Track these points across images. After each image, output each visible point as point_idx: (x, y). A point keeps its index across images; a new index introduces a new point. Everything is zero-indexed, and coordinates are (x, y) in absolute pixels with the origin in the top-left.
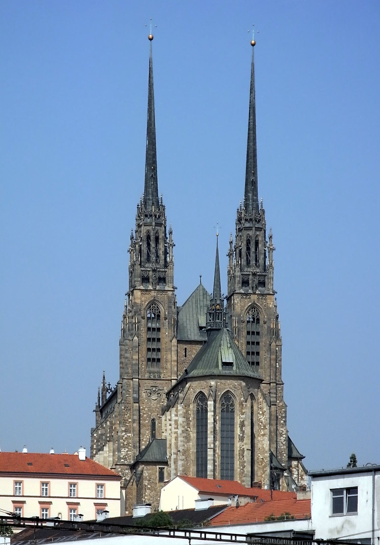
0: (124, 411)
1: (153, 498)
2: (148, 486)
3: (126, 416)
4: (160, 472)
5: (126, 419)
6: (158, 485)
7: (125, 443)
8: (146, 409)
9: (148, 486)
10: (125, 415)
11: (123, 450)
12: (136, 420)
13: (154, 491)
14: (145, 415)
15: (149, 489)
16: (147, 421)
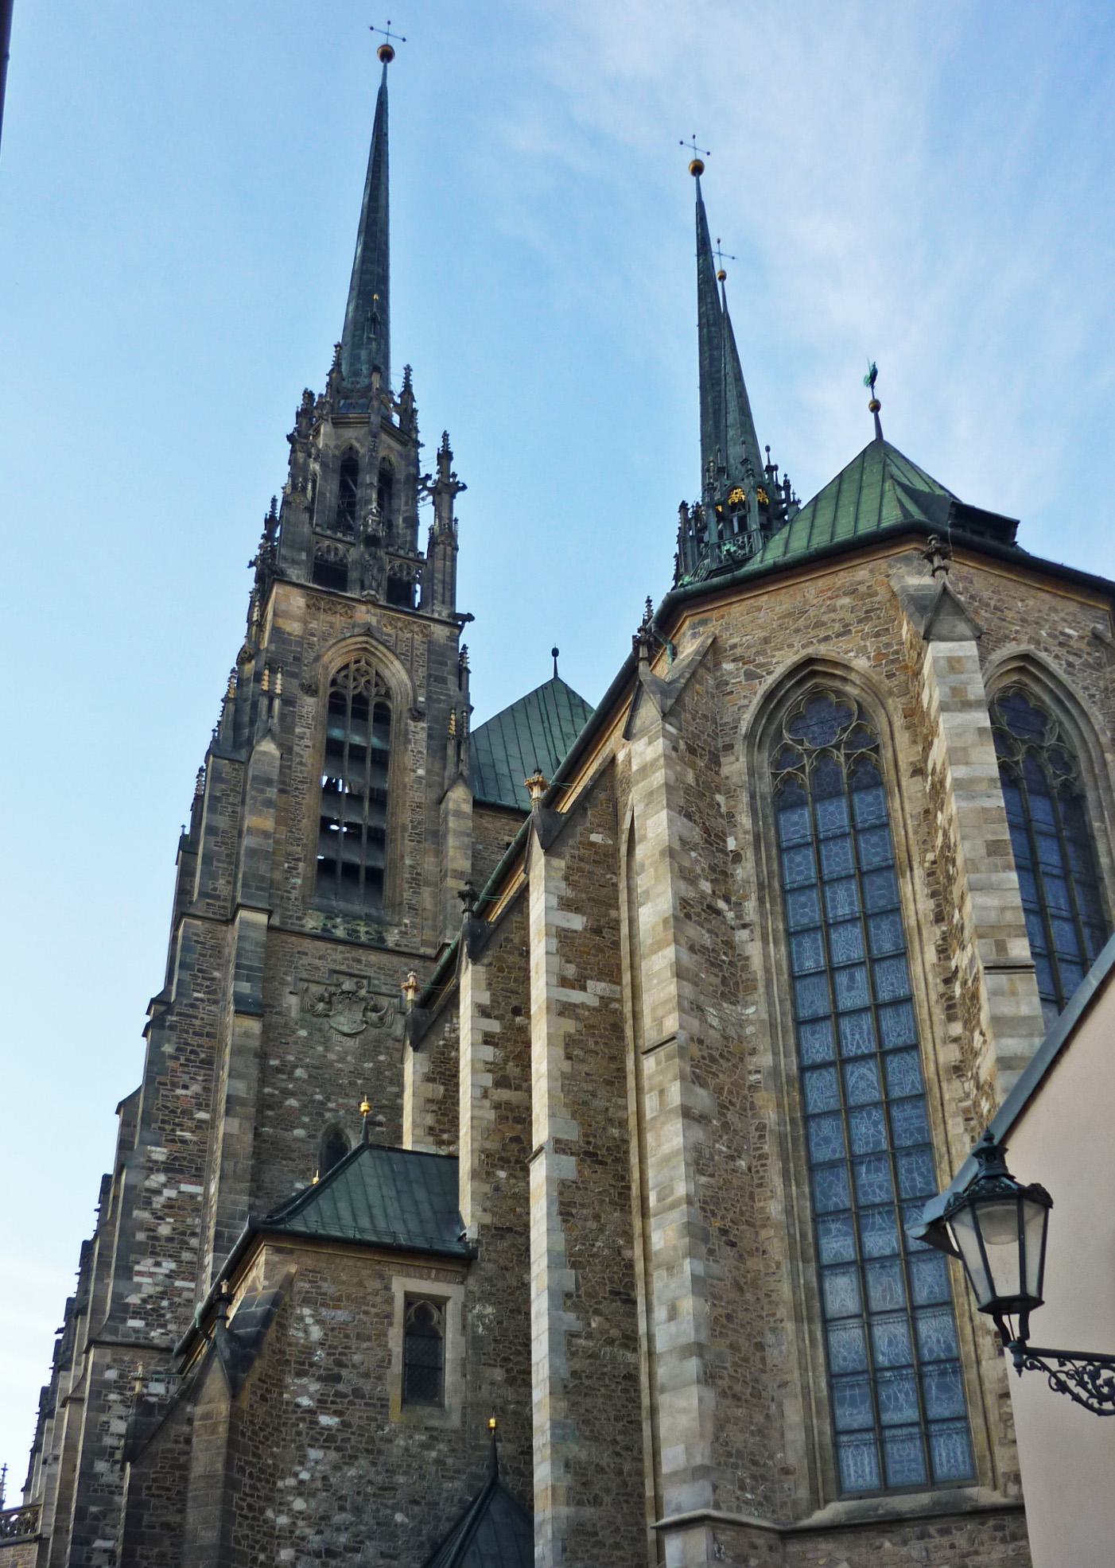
0: (170, 1064)
1: (357, 1511)
2: (325, 1420)
3: (179, 1092)
4: (409, 1332)
5: (183, 1105)
6: (395, 1414)
7: (164, 1230)
8: (299, 1072)
9: (325, 1420)
10: (175, 1085)
11: (146, 1265)
12: (242, 1102)
13: (363, 1462)
14: (292, 1102)
15: (327, 1439)
16: (299, 1132)
